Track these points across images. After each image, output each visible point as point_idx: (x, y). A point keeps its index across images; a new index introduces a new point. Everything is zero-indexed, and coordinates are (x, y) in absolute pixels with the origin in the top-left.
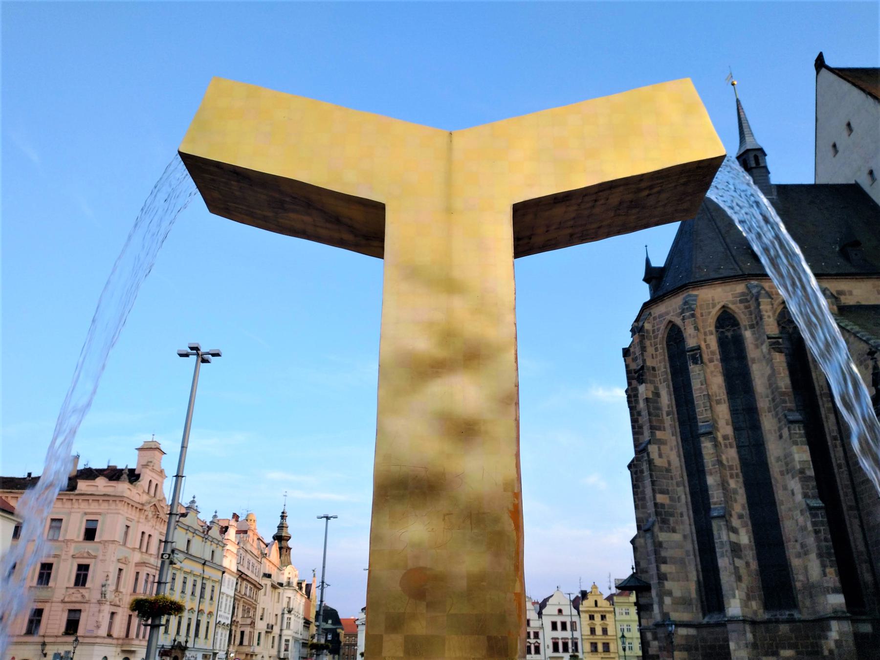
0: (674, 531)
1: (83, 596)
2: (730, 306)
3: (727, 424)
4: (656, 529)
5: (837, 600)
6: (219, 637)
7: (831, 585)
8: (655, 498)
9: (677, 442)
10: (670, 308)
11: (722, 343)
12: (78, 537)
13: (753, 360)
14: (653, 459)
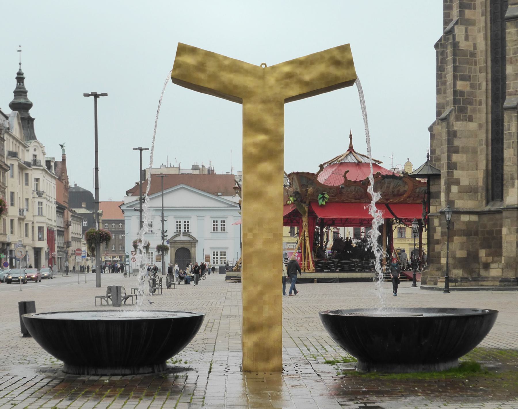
0: (470, 119)
4: (452, 119)
8: (455, 85)
9: (486, 24)
14: (459, 42)
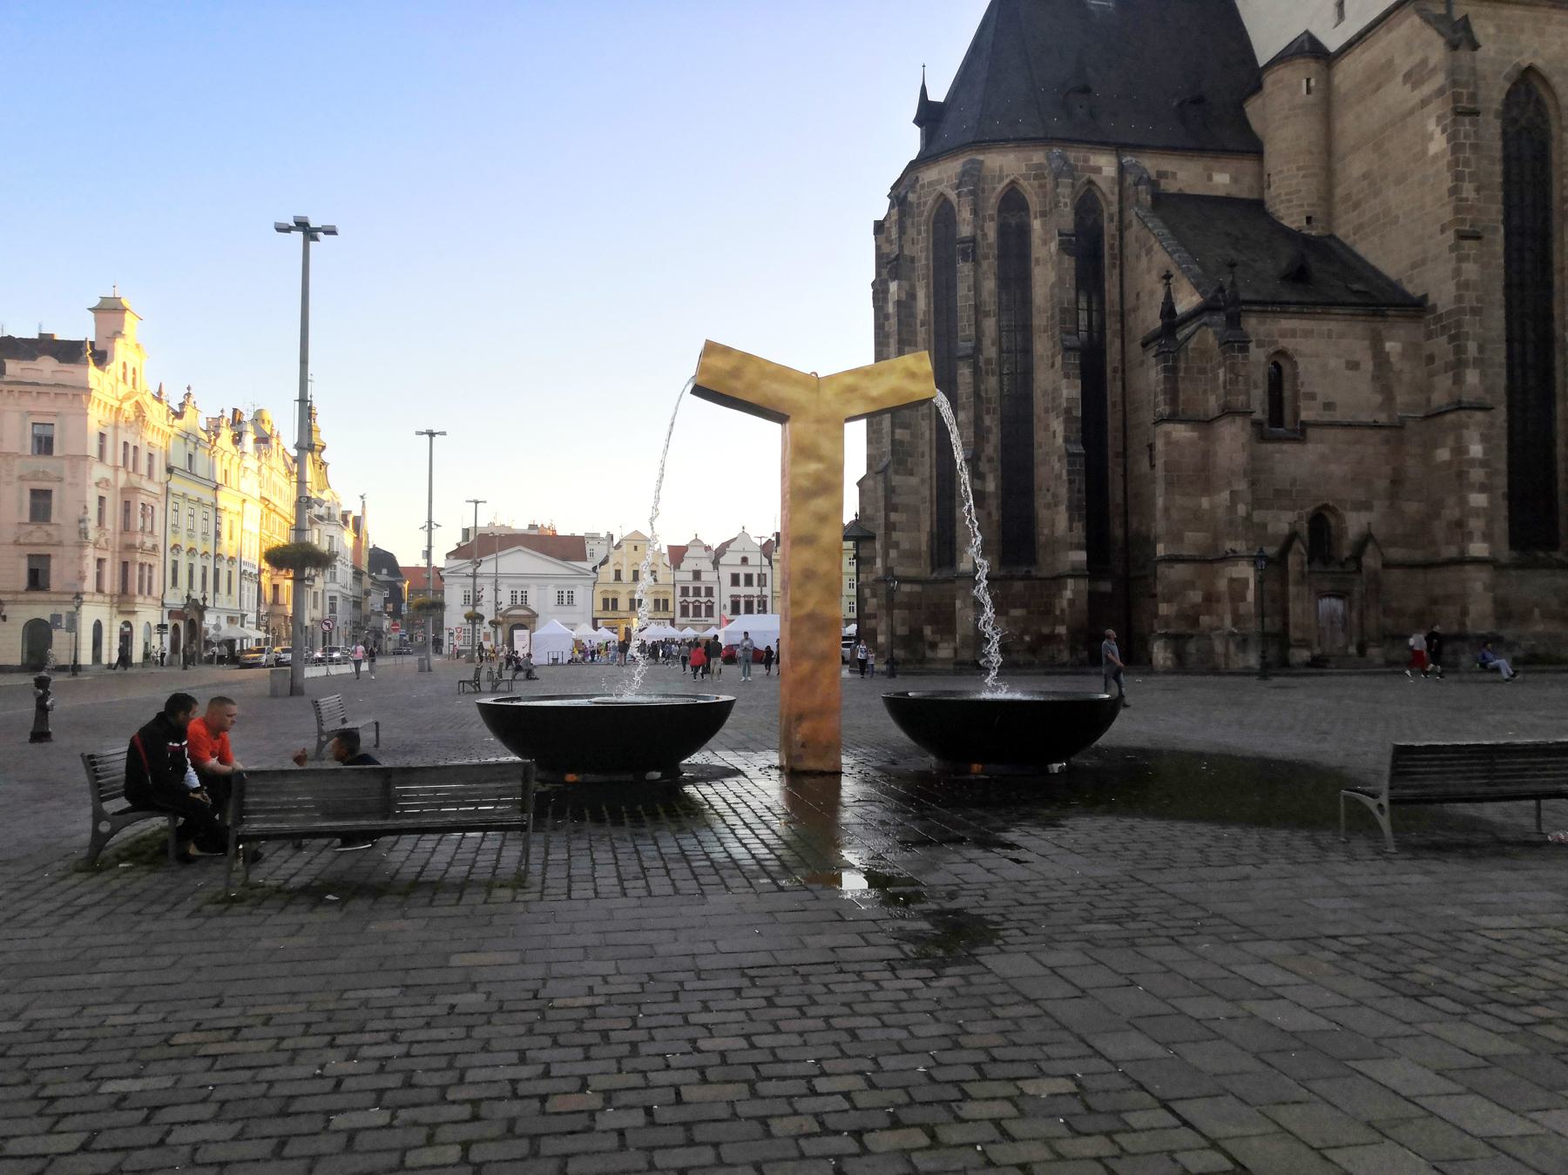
0: (911, 474)
1: (48, 534)
2: (1021, 181)
3: (993, 344)
4: (890, 471)
5: (1081, 556)
6: (245, 592)
7: (1076, 541)
10: (945, 174)
11: (1003, 232)
12: (24, 447)
13: (1037, 261)
